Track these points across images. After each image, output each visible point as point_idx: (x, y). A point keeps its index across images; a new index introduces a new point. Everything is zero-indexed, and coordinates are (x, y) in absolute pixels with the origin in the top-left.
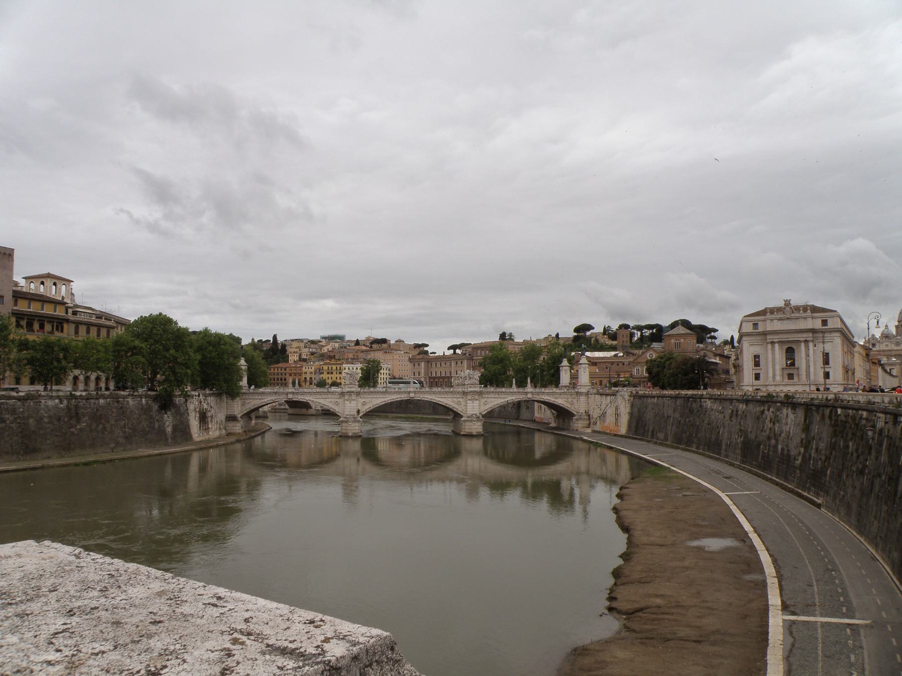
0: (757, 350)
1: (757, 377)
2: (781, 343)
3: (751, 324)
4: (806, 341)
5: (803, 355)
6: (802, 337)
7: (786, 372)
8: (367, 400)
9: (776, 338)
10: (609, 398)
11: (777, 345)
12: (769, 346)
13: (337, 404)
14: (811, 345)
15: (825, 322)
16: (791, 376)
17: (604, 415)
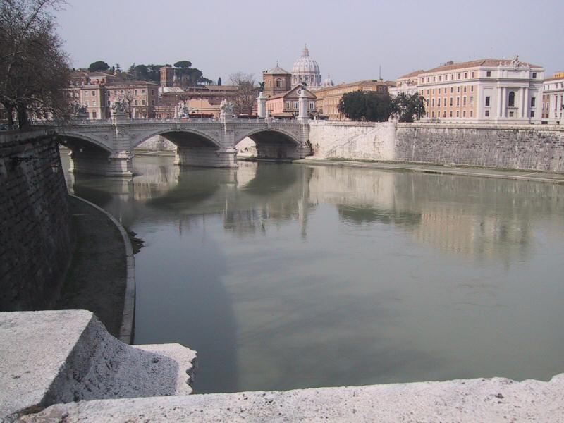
0: (487, 93)
1: (487, 114)
2: (508, 88)
3: (486, 72)
4: (525, 88)
5: (521, 99)
6: (522, 85)
7: (509, 111)
8: (136, 133)
9: (506, 84)
10: (351, 129)
11: (504, 90)
12: (499, 90)
13: (106, 138)
14: (527, 90)
15: (534, 75)
16: (511, 114)
17: (351, 142)
